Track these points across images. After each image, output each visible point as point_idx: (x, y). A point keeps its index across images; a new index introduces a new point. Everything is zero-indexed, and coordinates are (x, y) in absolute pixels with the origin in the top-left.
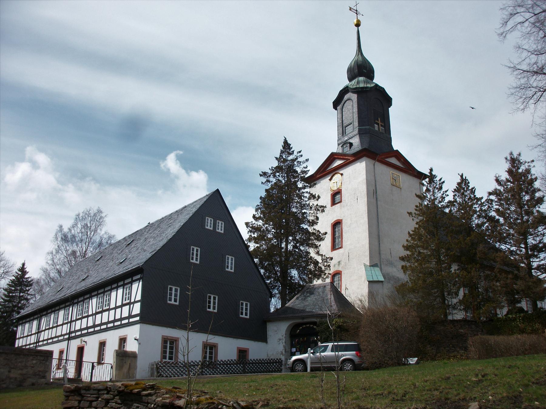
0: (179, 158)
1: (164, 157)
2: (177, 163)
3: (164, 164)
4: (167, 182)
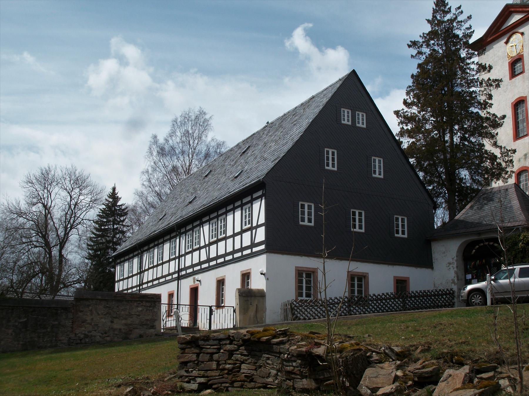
0: (310, 34)
1: (289, 34)
2: (306, 40)
3: (290, 42)
4: (296, 64)
